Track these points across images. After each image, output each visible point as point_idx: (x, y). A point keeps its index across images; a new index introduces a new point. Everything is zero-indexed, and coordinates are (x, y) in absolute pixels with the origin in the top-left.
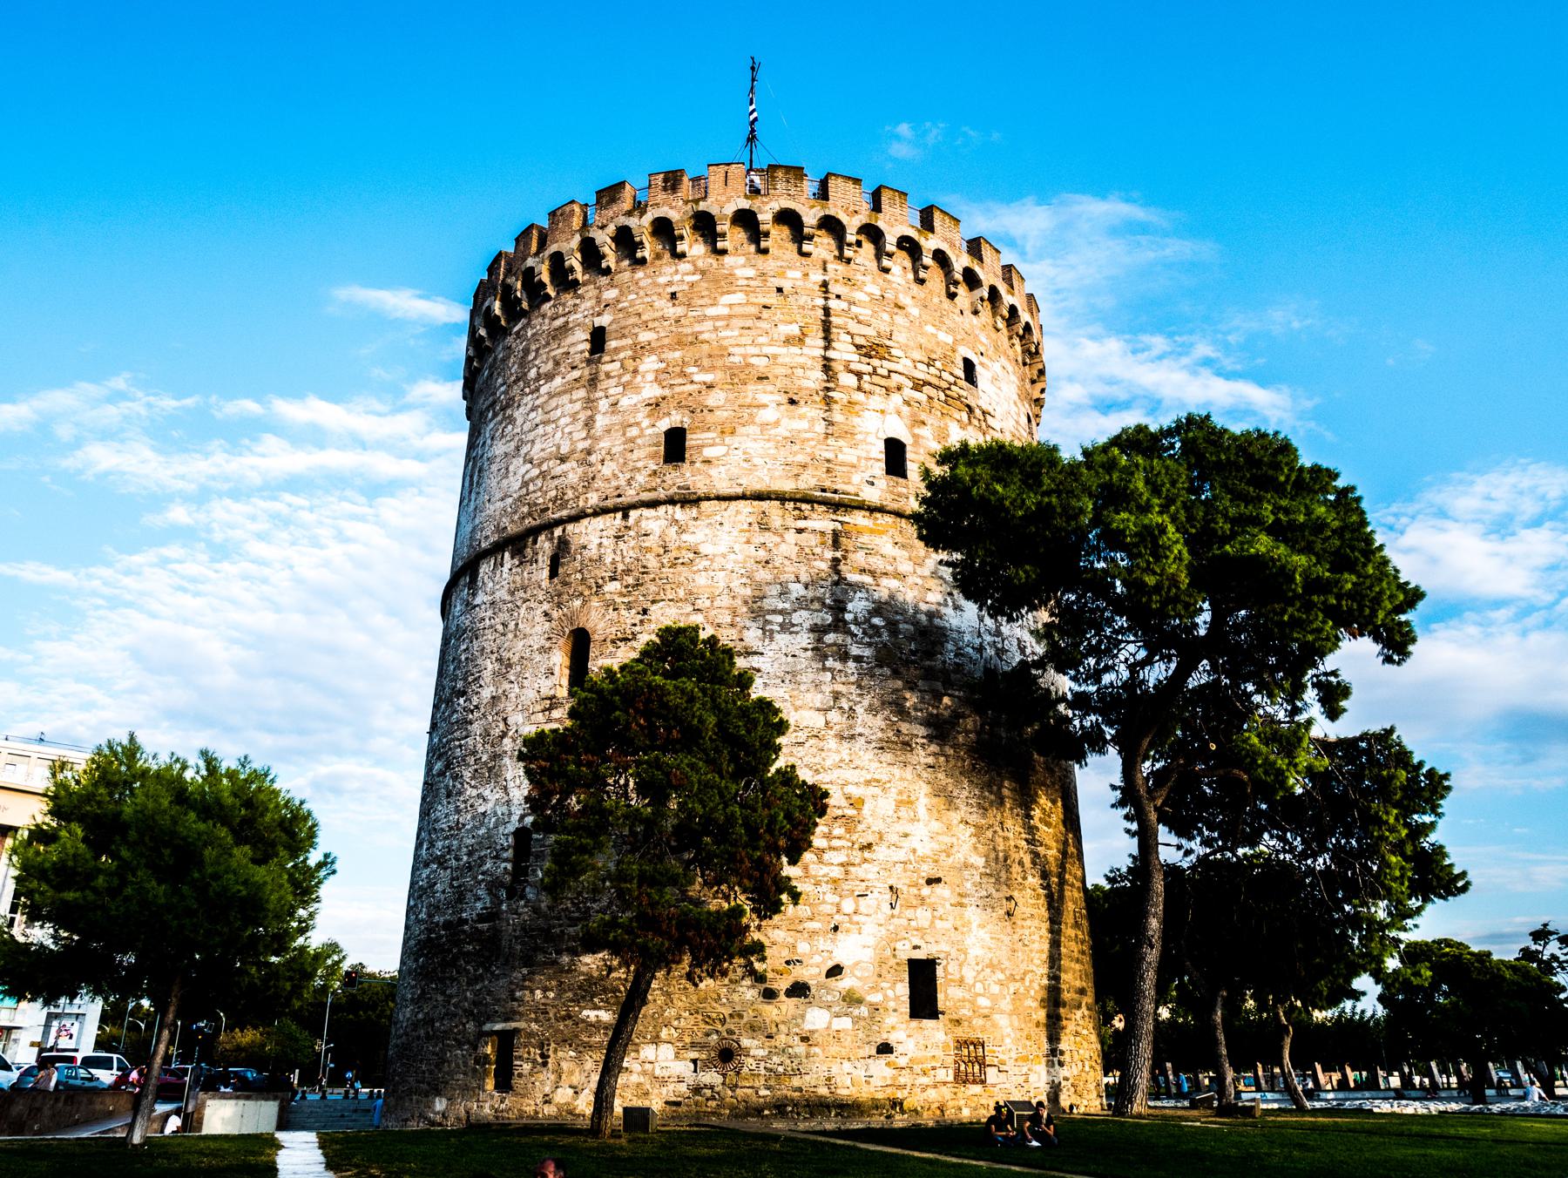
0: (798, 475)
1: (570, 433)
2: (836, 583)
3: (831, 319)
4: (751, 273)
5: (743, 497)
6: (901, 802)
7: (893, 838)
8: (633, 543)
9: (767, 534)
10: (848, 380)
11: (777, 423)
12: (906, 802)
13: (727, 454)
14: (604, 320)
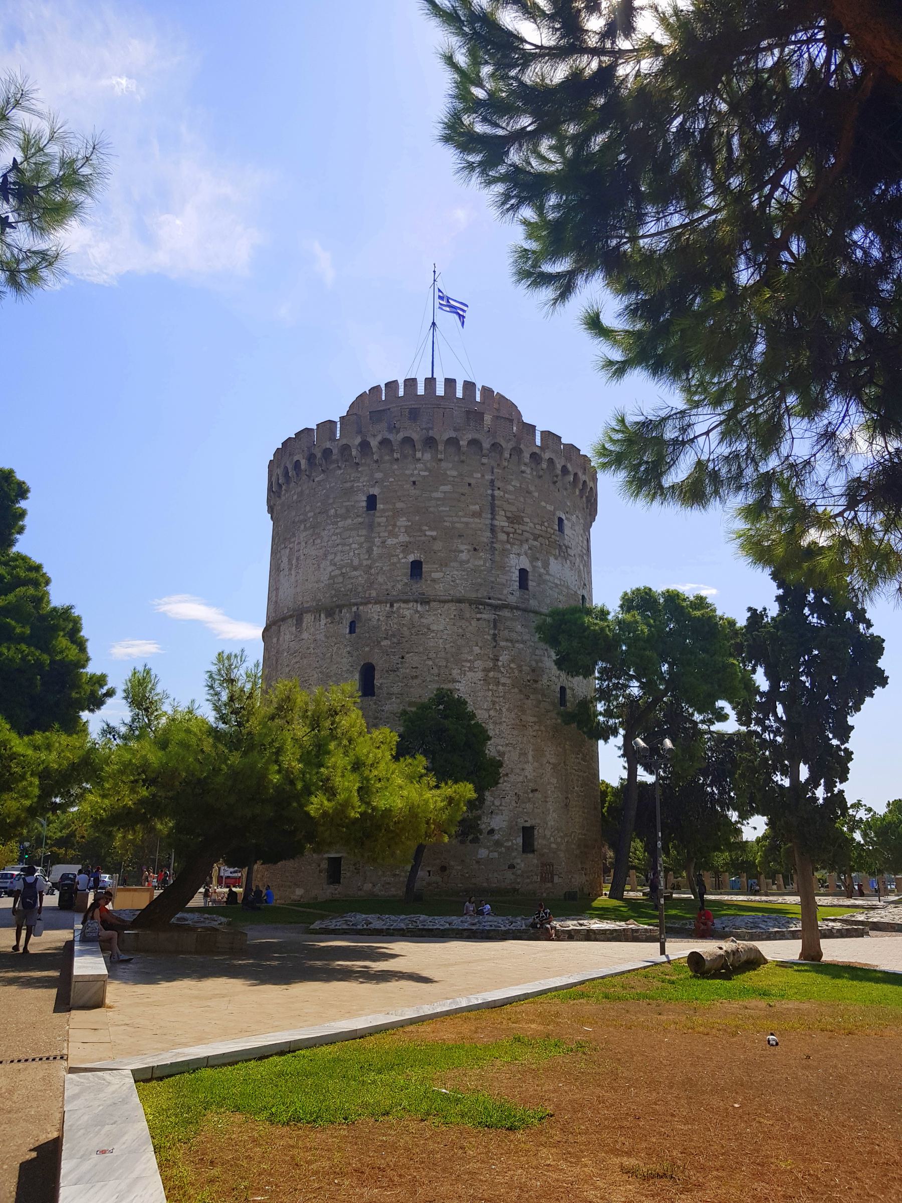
0: (478, 590)
1: (359, 554)
2: (495, 647)
3: (496, 502)
4: (455, 473)
5: (452, 601)
6: (522, 754)
7: (518, 771)
8: (396, 621)
9: (463, 621)
10: (503, 537)
11: (468, 562)
12: (523, 754)
13: (443, 577)
14: (375, 491)
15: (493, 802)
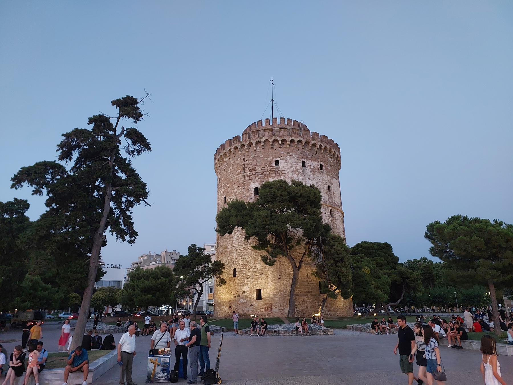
10: (248, 178)
15: (244, 281)
